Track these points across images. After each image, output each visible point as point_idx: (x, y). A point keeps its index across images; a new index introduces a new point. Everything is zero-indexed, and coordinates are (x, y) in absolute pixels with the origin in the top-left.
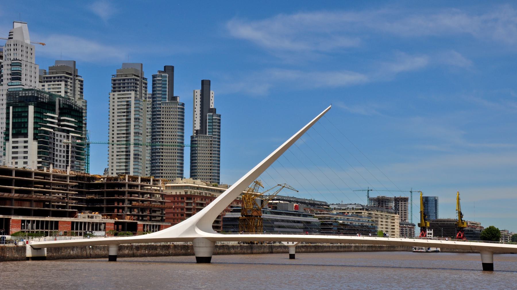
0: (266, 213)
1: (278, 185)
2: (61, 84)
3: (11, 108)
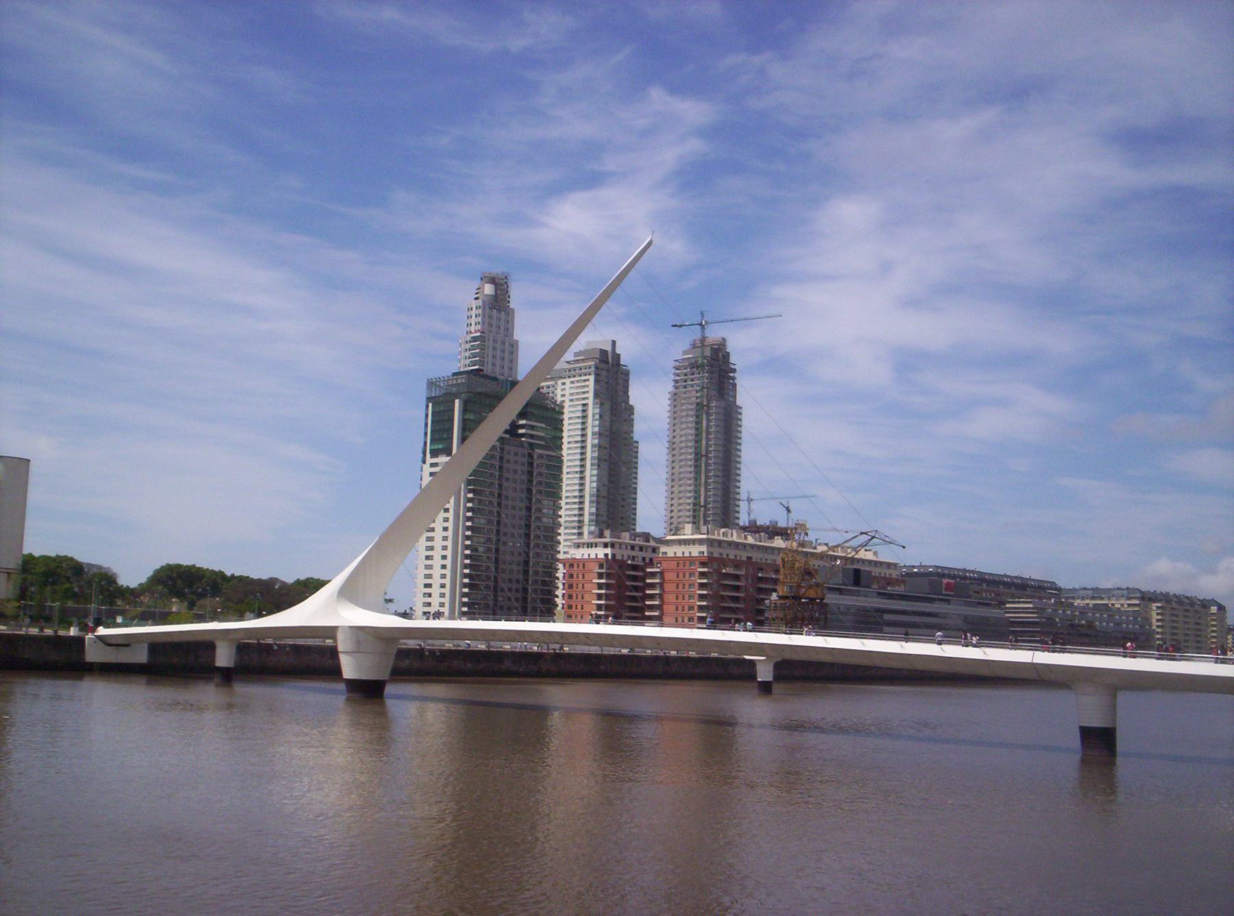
0: (866, 596)
1: (862, 533)
2: (588, 380)
3: (430, 405)
